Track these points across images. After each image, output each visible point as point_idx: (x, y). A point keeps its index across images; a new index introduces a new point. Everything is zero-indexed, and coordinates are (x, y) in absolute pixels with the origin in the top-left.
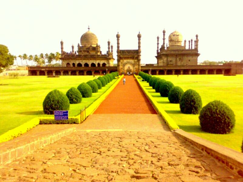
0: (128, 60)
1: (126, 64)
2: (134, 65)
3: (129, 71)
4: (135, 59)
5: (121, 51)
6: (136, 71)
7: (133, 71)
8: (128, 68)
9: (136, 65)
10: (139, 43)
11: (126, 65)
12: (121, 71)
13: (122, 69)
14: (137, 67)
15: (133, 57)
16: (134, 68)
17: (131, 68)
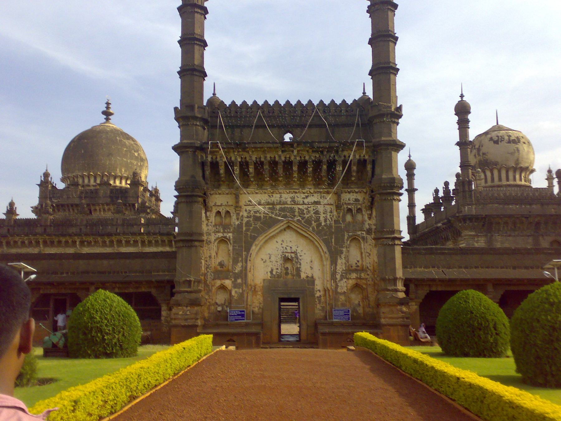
0: (287, 197)
1: (264, 224)
2: (332, 240)
3: (289, 296)
4: (347, 181)
5: (215, 104)
6: (356, 298)
7: (332, 293)
8: (276, 264)
9: (354, 239)
10: (383, 39)
11: (261, 239)
12: (221, 298)
13: (222, 272)
14: (361, 254)
15: (332, 164)
16: (341, 266)
17: (312, 264)
